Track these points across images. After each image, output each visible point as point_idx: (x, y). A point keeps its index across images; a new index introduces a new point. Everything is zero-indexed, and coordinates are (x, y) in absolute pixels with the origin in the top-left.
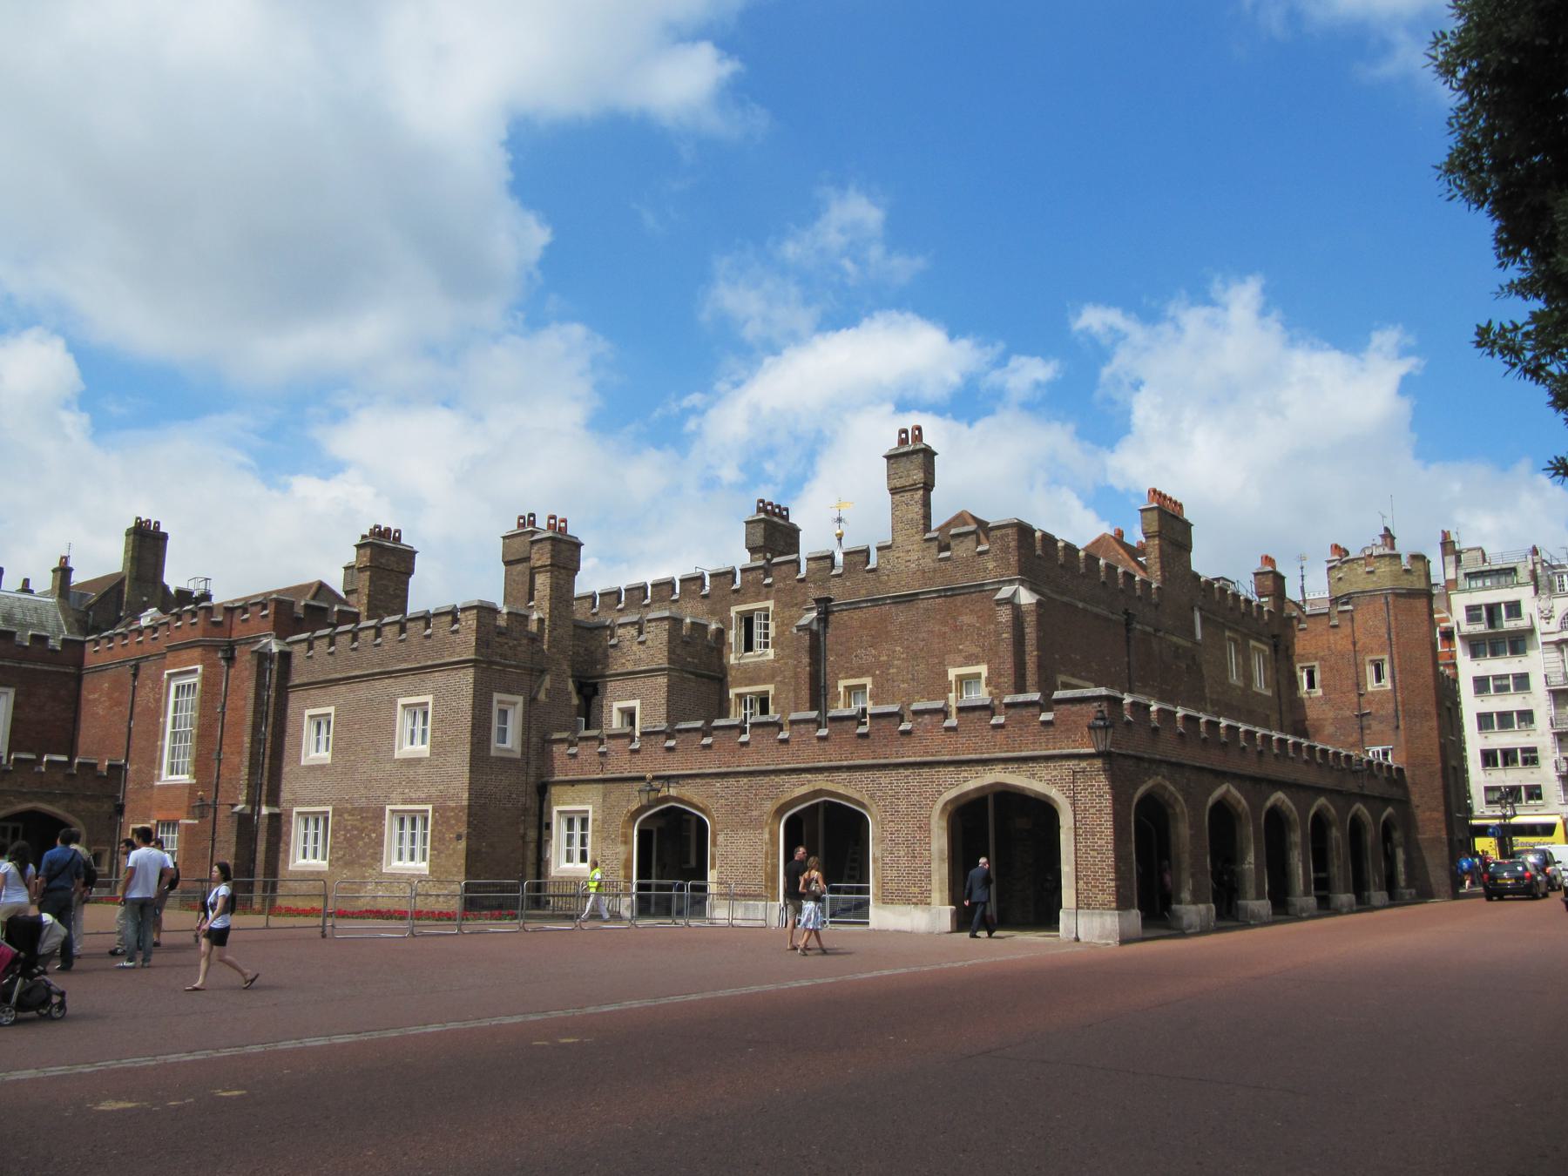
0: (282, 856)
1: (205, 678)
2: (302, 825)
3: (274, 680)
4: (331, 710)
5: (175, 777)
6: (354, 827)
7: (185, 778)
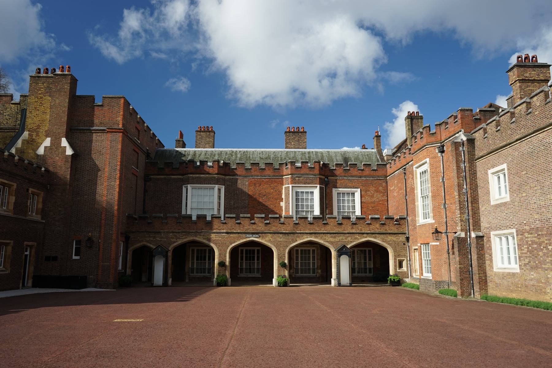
0: (487, 262)
1: (431, 165)
2: (498, 240)
3: (466, 157)
4: (505, 166)
5: (425, 220)
6: (533, 242)
7: (431, 221)
